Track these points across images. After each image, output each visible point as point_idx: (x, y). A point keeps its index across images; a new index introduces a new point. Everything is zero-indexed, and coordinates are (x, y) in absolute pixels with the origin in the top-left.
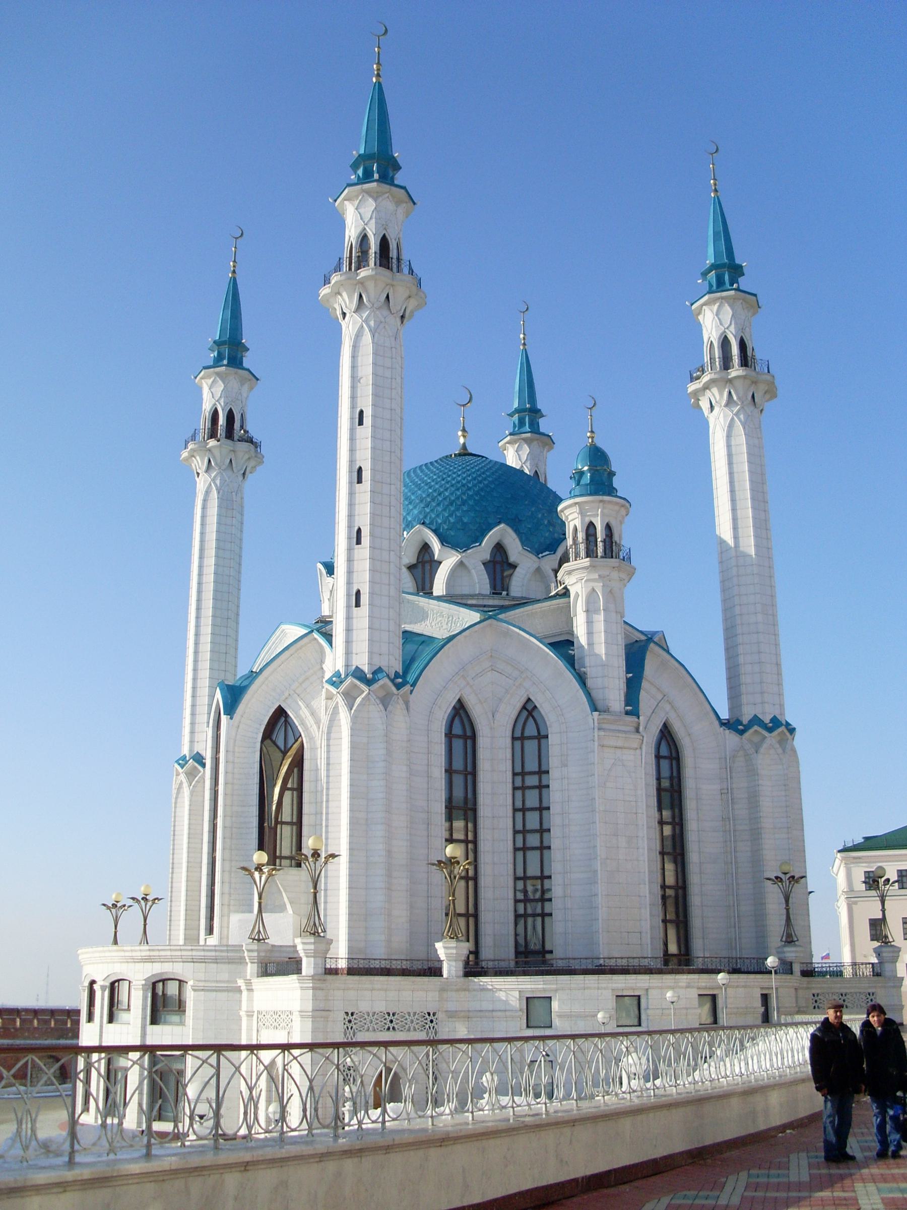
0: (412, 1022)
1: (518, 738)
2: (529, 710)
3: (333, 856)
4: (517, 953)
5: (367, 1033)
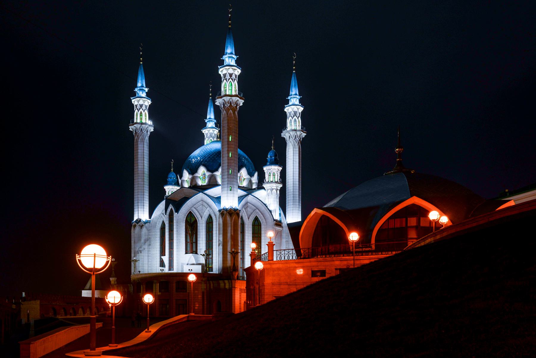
1: (254, 225)
2: (256, 219)
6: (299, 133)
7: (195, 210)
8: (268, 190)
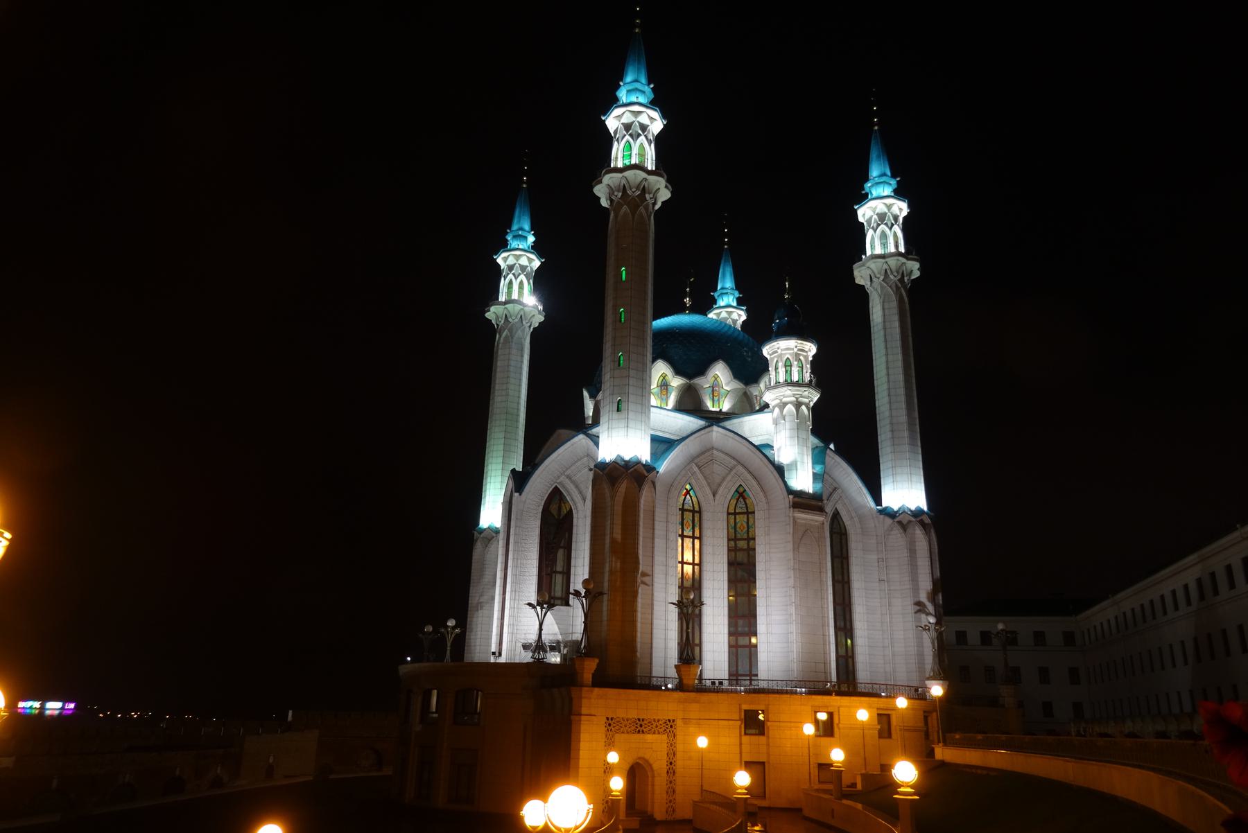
2: (741, 494)
3: (601, 594)
4: (730, 675)
7: (567, 481)
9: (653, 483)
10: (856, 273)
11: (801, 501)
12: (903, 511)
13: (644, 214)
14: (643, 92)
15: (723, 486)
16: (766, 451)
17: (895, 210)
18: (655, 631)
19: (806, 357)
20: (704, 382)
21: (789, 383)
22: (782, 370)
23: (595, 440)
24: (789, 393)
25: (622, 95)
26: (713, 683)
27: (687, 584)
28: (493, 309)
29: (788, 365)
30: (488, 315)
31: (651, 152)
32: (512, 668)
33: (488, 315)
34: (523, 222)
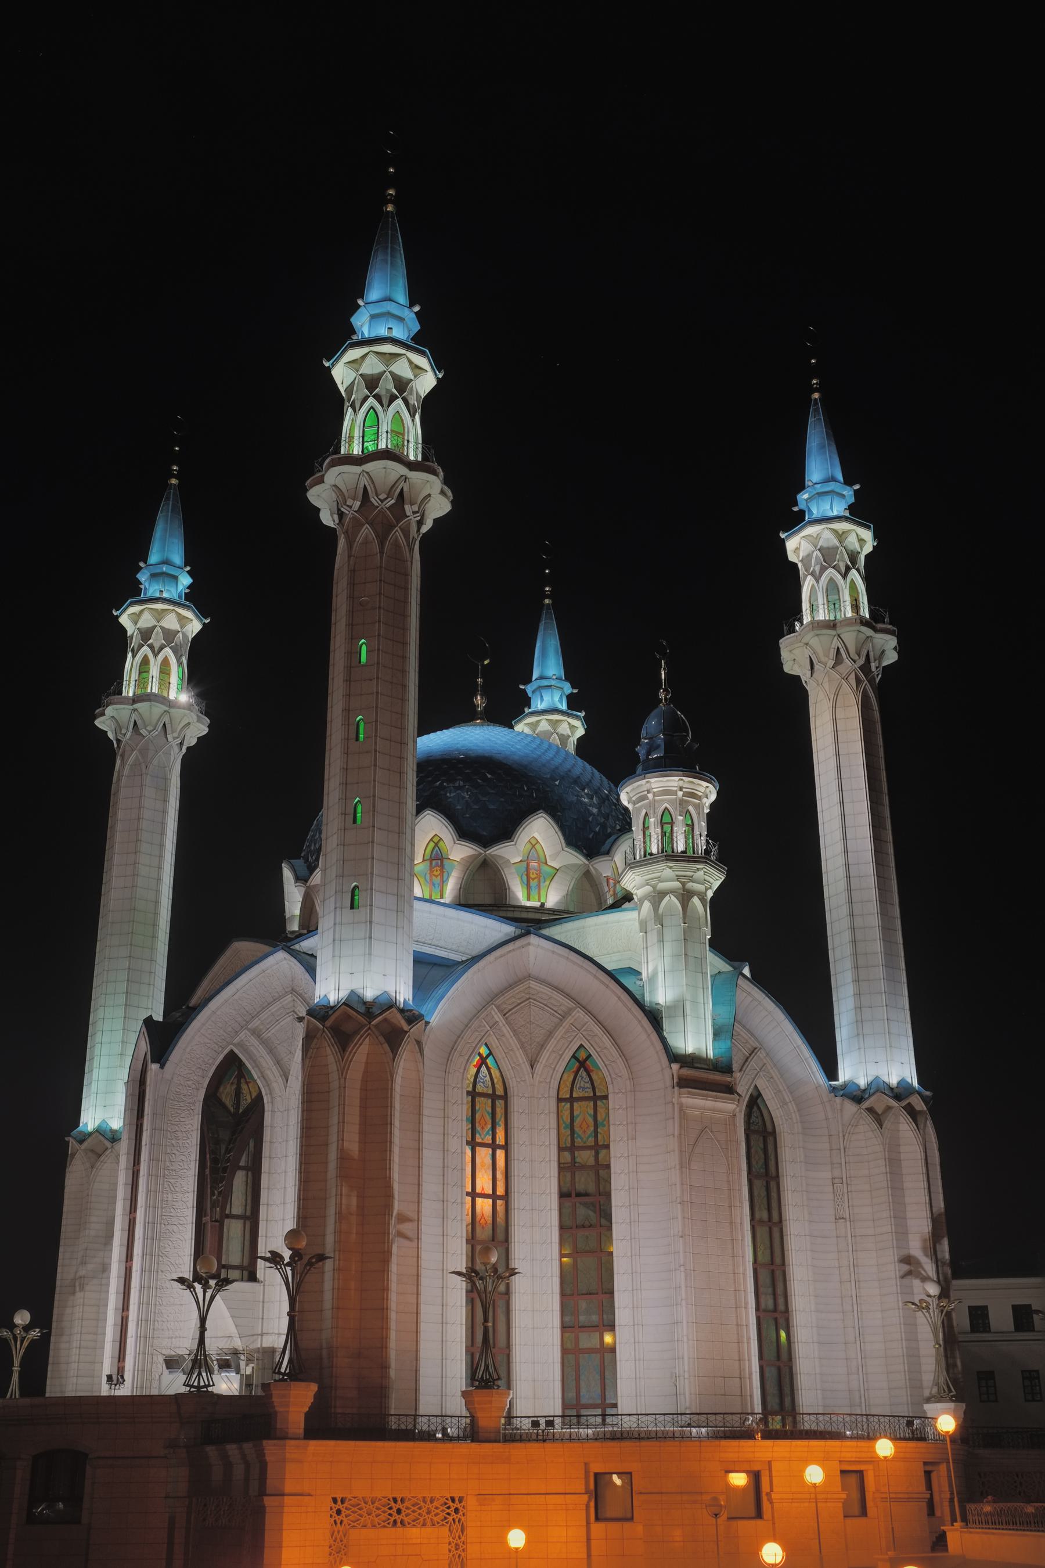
0: (429, 1513)
1: (566, 1100)
3: (322, 1258)
4: (565, 1406)
5: (364, 1531)
6: (850, 637)
7: (254, 1041)
8: (642, 901)
9: (419, 1043)
10: (784, 654)
11: (699, 1075)
12: (878, 1088)
13: (402, 540)
14: (401, 319)
15: (551, 1045)
16: (627, 981)
17: (852, 542)
18: (423, 1327)
19: (698, 807)
20: (511, 854)
21: (669, 855)
22: (655, 832)
23: (309, 963)
24: (668, 873)
25: (363, 323)
26: (536, 1424)
27: (484, 1233)
28: (110, 711)
29: (666, 822)
30: (98, 723)
31: (414, 428)
32: (145, 1407)
33: (98, 723)
34: (167, 549)
